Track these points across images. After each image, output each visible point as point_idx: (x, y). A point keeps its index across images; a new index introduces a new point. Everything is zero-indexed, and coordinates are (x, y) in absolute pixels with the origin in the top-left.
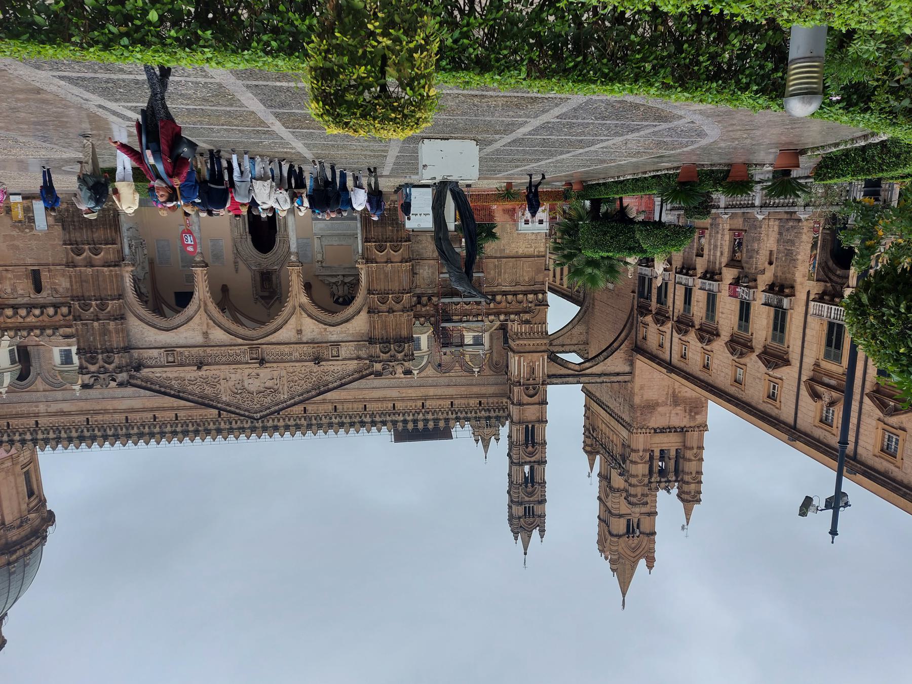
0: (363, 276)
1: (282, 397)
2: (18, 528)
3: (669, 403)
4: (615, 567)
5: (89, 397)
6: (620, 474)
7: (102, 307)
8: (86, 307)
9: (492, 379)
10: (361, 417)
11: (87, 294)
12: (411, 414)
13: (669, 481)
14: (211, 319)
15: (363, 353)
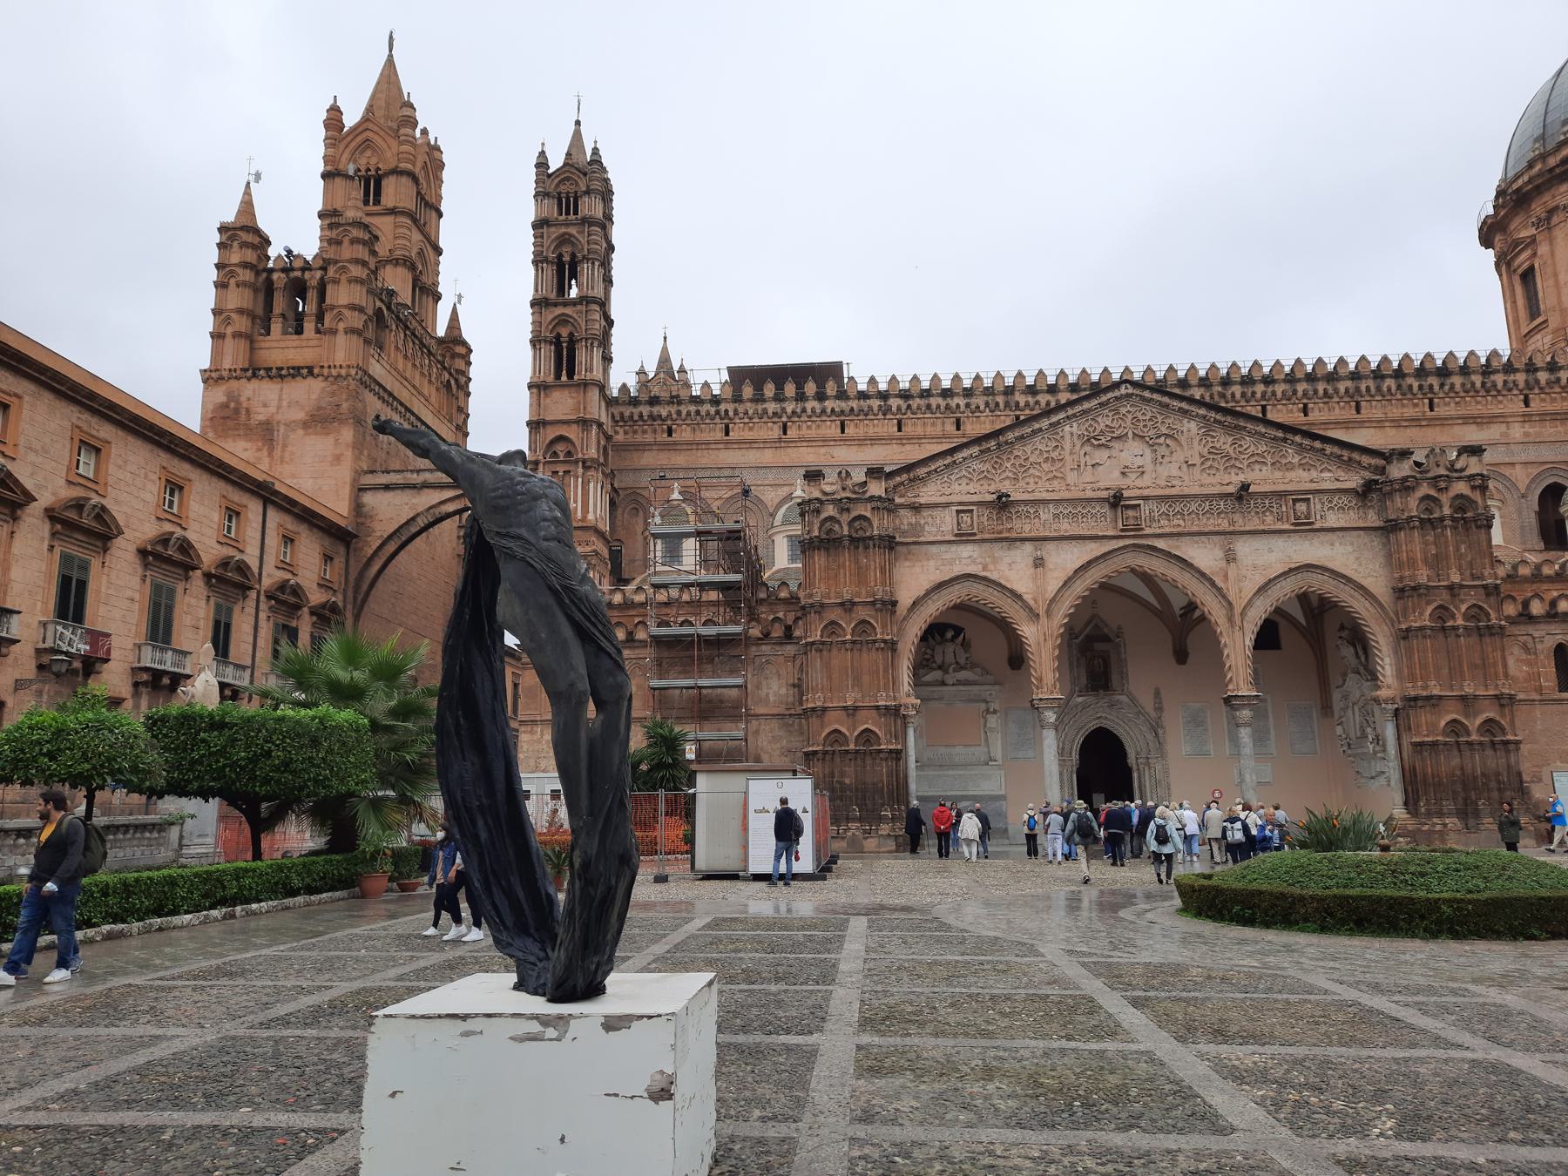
0: (906, 679)
1: (1075, 429)
2: (1556, 208)
3: (282, 429)
4: (406, 111)
6: (391, 293)
7: (1442, 613)
8: (1476, 613)
9: (644, 480)
10: (909, 407)
11: (1474, 639)
12: (809, 411)
13: (285, 270)
14: (1219, 590)
15: (907, 517)
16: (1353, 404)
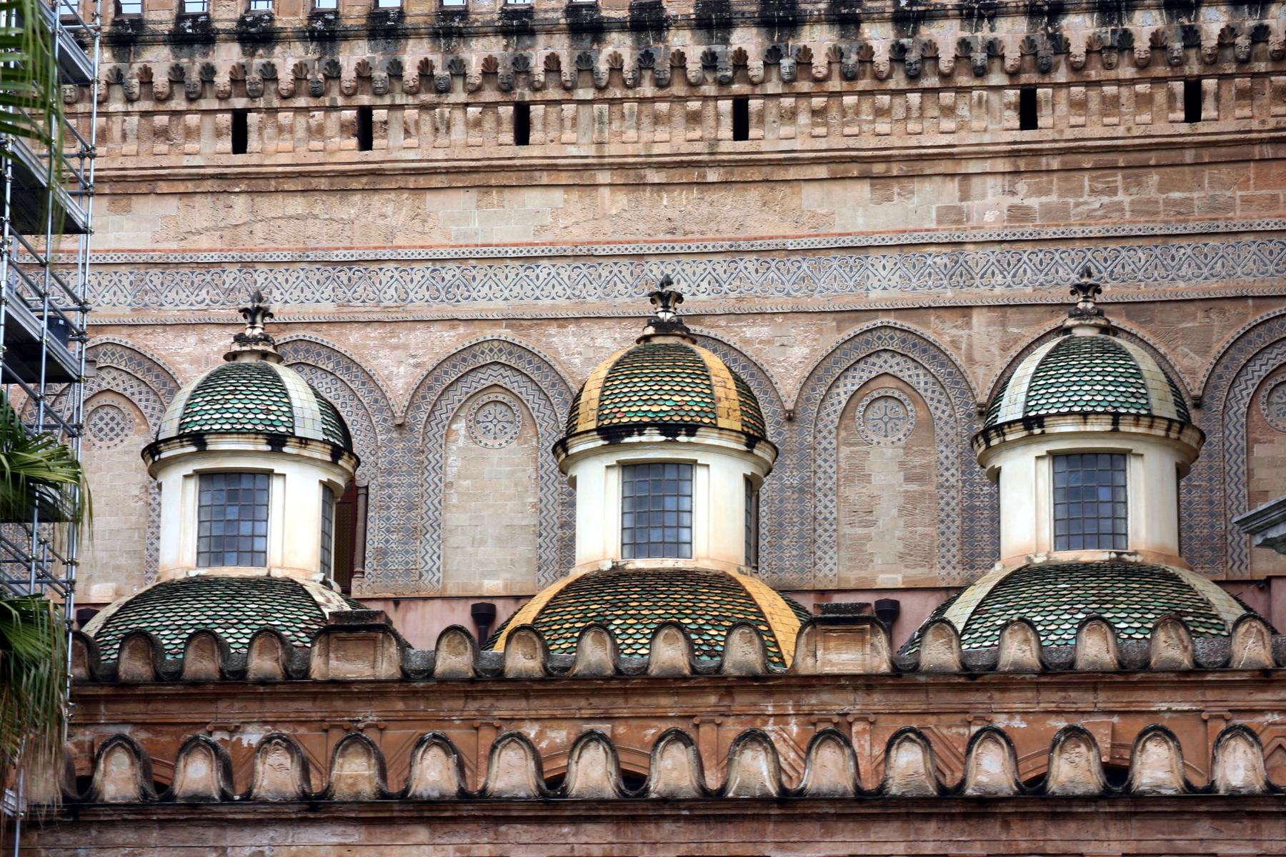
5: (721, 265)
16: (507, 111)
